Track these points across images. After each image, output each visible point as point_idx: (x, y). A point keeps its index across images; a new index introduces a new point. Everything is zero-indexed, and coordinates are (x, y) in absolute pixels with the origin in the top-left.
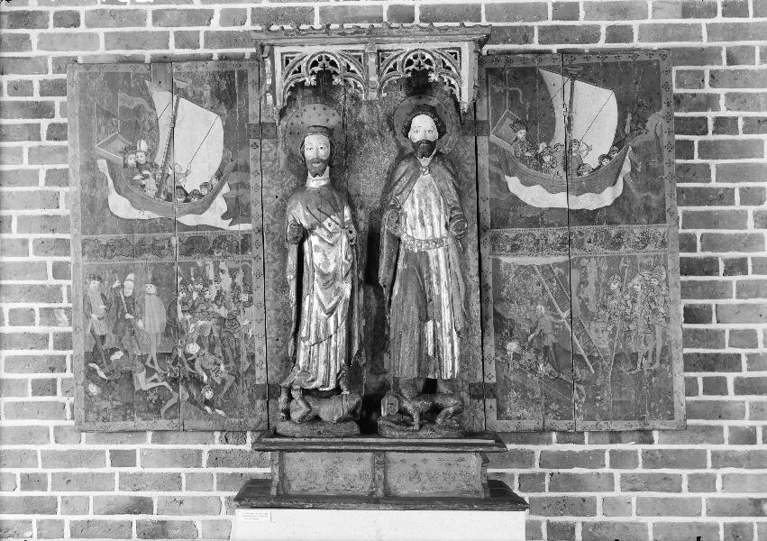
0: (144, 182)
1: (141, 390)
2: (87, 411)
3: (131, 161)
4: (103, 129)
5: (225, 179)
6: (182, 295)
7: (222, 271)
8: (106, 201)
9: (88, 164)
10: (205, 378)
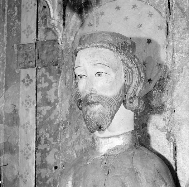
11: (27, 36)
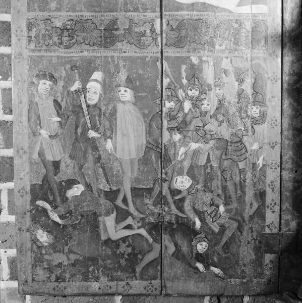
1: (109, 239)
2: (34, 266)
6: (169, 105)
7: (225, 72)
10: (198, 224)
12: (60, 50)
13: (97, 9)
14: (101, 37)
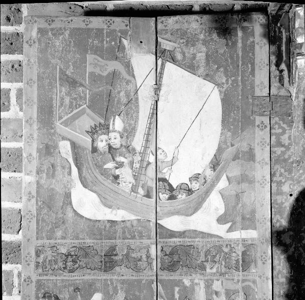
0: (117, 172)
3: (102, 145)
4: (67, 100)
5: (224, 169)
7: (217, 293)
8: (68, 196)
9: (47, 147)
11: (261, 90)
12: (65, 274)
13: (99, 237)
14: (101, 262)
